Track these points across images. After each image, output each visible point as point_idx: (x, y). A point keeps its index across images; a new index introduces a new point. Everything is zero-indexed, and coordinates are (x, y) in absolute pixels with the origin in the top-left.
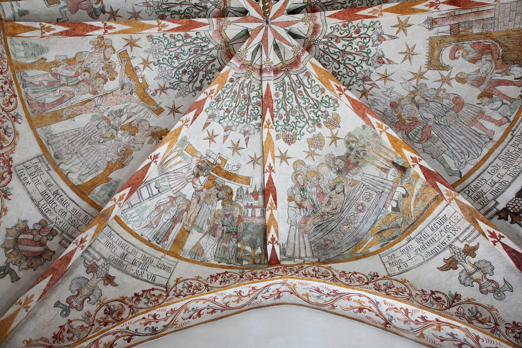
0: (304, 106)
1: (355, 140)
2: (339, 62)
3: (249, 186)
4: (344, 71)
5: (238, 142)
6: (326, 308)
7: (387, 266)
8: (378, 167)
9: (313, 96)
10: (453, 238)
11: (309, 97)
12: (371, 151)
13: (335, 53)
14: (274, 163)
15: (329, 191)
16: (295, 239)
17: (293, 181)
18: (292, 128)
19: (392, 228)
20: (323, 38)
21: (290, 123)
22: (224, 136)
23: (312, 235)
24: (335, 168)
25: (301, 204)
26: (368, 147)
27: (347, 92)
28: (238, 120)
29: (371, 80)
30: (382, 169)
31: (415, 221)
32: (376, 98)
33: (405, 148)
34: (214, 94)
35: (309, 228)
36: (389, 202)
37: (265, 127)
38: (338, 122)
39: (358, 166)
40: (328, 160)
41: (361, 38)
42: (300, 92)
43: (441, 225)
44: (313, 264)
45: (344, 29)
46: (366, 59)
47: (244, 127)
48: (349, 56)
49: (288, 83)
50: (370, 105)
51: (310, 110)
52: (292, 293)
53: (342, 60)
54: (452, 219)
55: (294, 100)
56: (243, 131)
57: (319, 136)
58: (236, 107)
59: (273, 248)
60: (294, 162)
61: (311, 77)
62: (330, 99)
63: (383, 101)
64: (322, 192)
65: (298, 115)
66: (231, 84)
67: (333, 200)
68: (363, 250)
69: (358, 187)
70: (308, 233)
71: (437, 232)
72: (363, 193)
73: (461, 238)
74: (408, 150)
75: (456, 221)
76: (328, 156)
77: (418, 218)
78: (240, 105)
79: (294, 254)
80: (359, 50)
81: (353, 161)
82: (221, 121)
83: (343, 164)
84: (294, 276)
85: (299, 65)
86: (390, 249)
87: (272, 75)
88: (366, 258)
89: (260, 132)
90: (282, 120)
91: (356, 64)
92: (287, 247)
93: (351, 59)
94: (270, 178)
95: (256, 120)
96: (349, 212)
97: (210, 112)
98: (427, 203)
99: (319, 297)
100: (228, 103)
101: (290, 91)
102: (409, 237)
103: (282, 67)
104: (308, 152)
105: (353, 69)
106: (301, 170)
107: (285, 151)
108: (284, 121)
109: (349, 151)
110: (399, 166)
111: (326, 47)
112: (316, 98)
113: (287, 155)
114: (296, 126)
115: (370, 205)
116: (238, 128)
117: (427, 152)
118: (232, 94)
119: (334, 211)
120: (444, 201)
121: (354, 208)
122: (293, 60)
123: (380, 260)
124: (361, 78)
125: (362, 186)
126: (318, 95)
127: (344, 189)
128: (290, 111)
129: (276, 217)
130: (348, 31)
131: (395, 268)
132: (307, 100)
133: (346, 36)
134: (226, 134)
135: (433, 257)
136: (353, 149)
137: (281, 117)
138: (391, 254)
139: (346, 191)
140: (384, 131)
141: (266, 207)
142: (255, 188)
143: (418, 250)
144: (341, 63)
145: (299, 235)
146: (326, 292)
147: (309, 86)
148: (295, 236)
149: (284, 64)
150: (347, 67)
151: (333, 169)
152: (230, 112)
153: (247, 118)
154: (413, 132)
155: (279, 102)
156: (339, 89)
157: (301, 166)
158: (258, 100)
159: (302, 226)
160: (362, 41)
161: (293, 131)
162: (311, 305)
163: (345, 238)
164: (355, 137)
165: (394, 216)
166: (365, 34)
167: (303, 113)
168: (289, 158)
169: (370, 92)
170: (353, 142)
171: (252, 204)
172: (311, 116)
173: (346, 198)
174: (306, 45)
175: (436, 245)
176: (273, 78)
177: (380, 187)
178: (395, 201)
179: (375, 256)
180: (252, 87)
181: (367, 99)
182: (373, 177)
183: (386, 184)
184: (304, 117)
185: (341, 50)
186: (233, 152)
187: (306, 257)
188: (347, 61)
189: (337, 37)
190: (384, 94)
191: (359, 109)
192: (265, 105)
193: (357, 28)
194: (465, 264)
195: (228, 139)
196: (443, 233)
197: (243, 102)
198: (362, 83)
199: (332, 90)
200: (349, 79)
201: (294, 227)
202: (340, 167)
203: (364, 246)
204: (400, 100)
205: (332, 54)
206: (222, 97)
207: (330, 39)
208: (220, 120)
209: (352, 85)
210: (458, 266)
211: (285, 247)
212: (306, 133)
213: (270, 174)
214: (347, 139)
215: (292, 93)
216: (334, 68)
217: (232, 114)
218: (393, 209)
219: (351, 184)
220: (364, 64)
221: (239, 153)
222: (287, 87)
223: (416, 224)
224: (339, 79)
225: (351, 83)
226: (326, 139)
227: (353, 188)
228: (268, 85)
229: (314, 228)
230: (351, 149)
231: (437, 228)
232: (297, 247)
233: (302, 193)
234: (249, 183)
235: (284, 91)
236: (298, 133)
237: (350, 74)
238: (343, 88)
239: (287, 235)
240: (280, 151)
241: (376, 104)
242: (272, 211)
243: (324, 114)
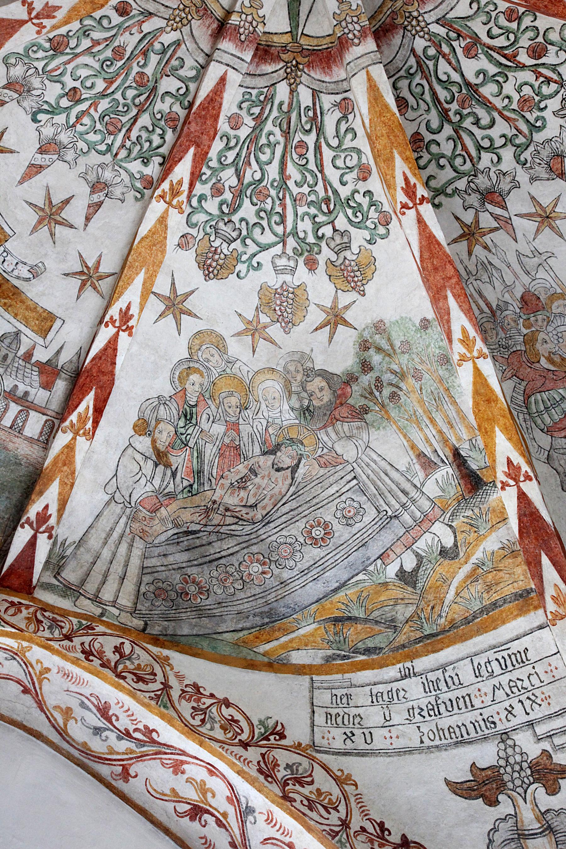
0: (295, 190)
1: (387, 347)
2: (444, 115)
3: (40, 341)
4: (447, 148)
5: (67, 202)
6: (104, 770)
7: (320, 719)
8: (413, 447)
9: (333, 175)
10: (521, 718)
11: (322, 171)
12: (414, 397)
13: (446, 84)
14: (141, 310)
15: (257, 451)
16: (105, 543)
17: (172, 382)
18: (235, 234)
19: (377, 622)
20: (437, 22)
21: (236, 218)
22: (31, 165)
23: (157, 551)
24: (301, 400)
25: (165, 454)
26: (411, 381)
27: (427, 210)
28: (92, 137)
29: (505, 208)
30: (421, 455)
31: (443, 632)
32: (495, 261)
33: (505, 430)
34: (53, 22)
35: (157, 527)
36: (398, 551)
37: (162, 197)
38: (365, 280)
39: (362, 419)
40: (292, 368)
41: (539, 75)
42: (302, 144)
43: (504, 669)
44: (124, 630)
45: (506, 24)
46: (520, 140)
47: (102, 166)
48: (481, 112)
49: (281, 104)
50: (469, 273)
51: (305, 209)
52: (26, 691)
53: (457, 113)
54: (539, 668)
55: (276, 163)
56: (92, 177)
57: (298, 292)
58: (103, 95)
59: (32, 544)
60: (199, 332)
61: (351, 117)
62: (372, 204)
63: (509, 278)
64: (237, 448)
65: (268, 207)
66: (116, 19)
67: (257, 480)
68: (275, 649)
69: (337, 476)
70: (150, 540)
71: (487, 687)
72: (343, 498)
73: (541, 729)
74: (510, 439)
75: (546, 679)
76: (296, 357)
77: (453, 625)
78: (118, 96)
79: (83, 582)
80: (515, 106)
81: (356, 400)
82: (40, 117)
83: (327, 396)
84: (55, 645)
85: (335, 69)
86: (347, 676)
87: (248, 56)
88: (273, 674)
89: (139, 204)
90: (219, 199)
91: (486, 143)
92: (74, 554)
94: (112, 347)
95: (146, 162)
96: (284, 533)
97: (18, 71)
98: (495, 597)
99: (97, 731)
100: (83, 73)
101: (277, 131)
102: (408, 664)
103: (284, 49)
104: (249, 322)
105: (474, 153)
106: (208, 361)
107: (188, 290)
108: (221, 204)
109: (357, 369)
110: (468, 468)
111: (432, 52)
112: (336, 184)
113: (188, 304)
114: (249, 236)
115: (346, 536)
116: (82, 160)
117: (556, 465)
118: (108, 53)
119: (244, 511)
120: (541, 611)
121: (301, 525)
122: (324, 44)
123: (307, 694)
124: (482, 187)
125: (349, 477)
126: (345, 179)
127: (297, 465)
128: (250, 185)
129: (79, 458)
130: (512, 37)
131: (338, 733)
132: (309, 178)
133: (500, 50)
134: (39, 159)
135: (446, 747)
136: (371, 369)
137: (217, 191)
138: (344, 691)
139: (301, 471)
140: (473, 359)
141: (63, 420)
142: (58, 352)
143: (417, 711)
144: (449, 121)
145: (122, 536)
146: (123, 723)
147: (334, 142)
148: (109, 535)
149: (295, 40)
150: (460, 138)
151: (294, 398)
152: (79, 101)
153: (123, 146)
154: (545, 396)
155: (232, 143)
156: (410, 191)
157: (214, 351)
158: (177, 108)
159: (141, 515)
160: (537, 84)
161: (233, 246)
162: (65, 746)
163: (242, 595)
164: (389, 339)
165: (397, 593)
166: (554, 70)
167: (284, 209)
168: (189, 313)
169: (487, 239)
170: (379, 349)
171: (26, 393)
172: (301, 226)
173: (293, 489)
174: (382, 18)
175: (469, 717)
176: (244, 67)
177: (393, 502)
178: (417, 555)
179: (300, 678)
180: (174, 63)
181: (470, 253)
182: (388, 468)
183: (414, 501)
184: (283, 221)
185: (468, 84)
186: (40, 222)
187: (114, 603)
188: (467, 123)
189: (476, 39)
190: (520, 263)
191: (436, 269)
192: (188, 135)
193: (540, 39)
194: (520, 801)
195: (40, 180)
196: (500, 694)
197: (130, 93)
198: (476, 204)
199: (389, 185)
201: (118, 509)
202: (316, 403)
203: (284, 639)
204: (553, 297)
205: (439, 80)
206: (73, 43)
207: (453, 35)
208: (40, 111)
210: (501, 797)
211: (68, 552)
212: (267, 267)
213: (118, 333)
214: (366, 334)
215: (278, 136)
216: (423, 125)
217: (84, 113)
218: (402, 574)
219: (322, 460)
220: (508, 154)
221: (52, 235)
222: (275, 113)
223: (441, 641)
224: (422, 162)
225: (449, 191)
226: (312, 308)
227: (322, 471)
228: (223, 80)
229: (171, 532)
230: (366, 367)
231: (492, 674)
232: (100, 566)
233: (181, 424)
234: (44, 332)
235: (260, 121)
236: (244, 258)
237: (458, 161)
238: (421, 191)
239: (90, 521)
240: (173, 284)
241: (485, 278)
242: (74, 439)
243: (338, 240)
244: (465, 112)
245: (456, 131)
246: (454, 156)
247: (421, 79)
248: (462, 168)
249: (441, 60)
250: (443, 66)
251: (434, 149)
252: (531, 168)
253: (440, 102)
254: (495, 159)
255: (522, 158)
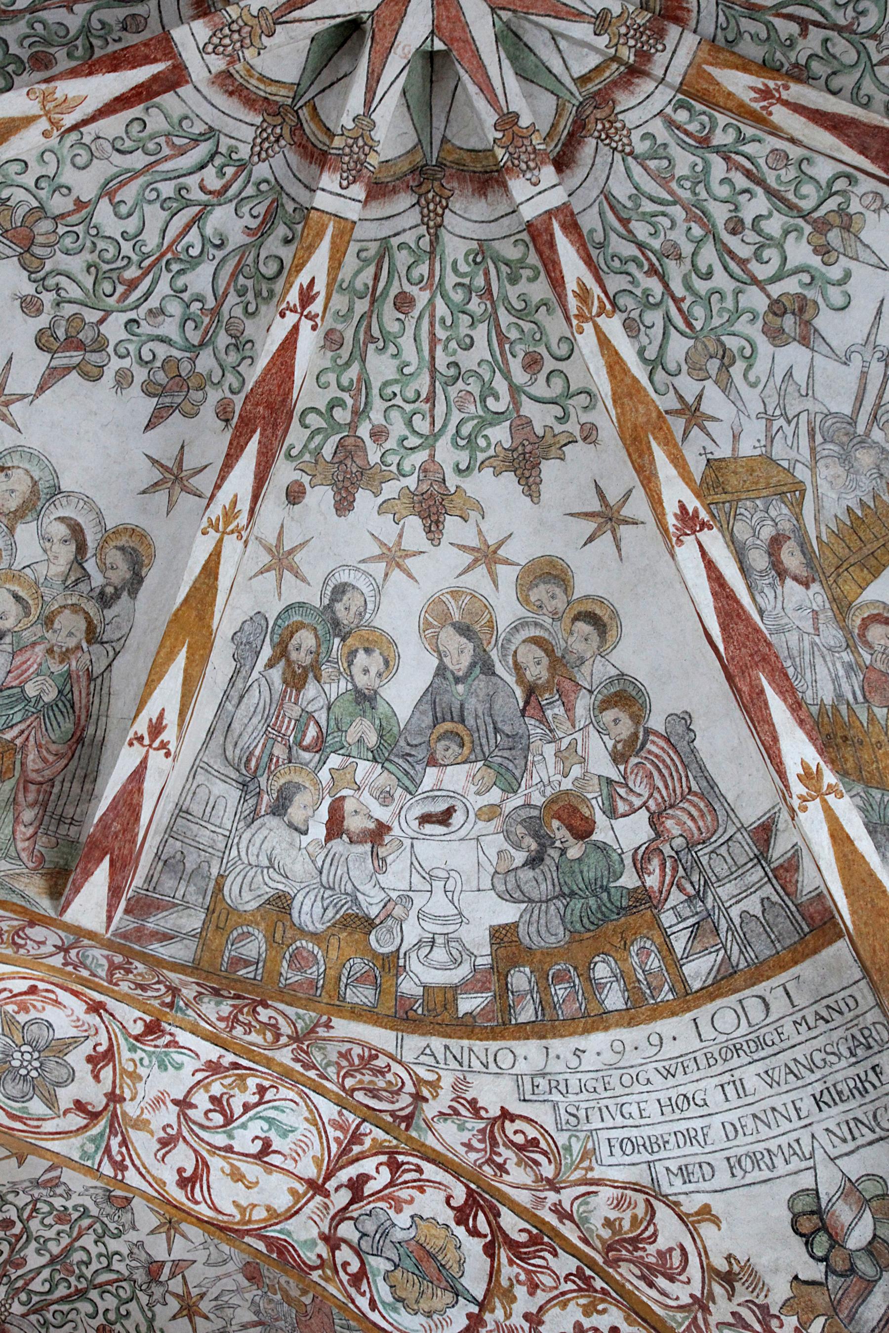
2: (81, 1294)
32: (214, 1292)
41: (30, 1217)
48: (78, 1256)
80: (67, 1228)
91: (104, 1262)
93: (85, 1258)
111: (23, 1297)
150: (101, 1285)
169: (194, 1292)
181: (207, 1318)
188: (88, 1273)
198: (162, 1289)
200: (133, 1306)
205: (49, 1292)
209: (154, 1315)
220: (113, 1245)
237: (121, 1292)
244: (77, 1271)
245: (95, 1287)
246: (118, 1296)
247: (48, 1311)
248: (129, 1292)
249: (30, 1287)
250: (36, 1286)
251: (112, 1316)
252: (123, 1226)
253: (69, 1296)
254: (117, 1257)
255: (115, 1231)
